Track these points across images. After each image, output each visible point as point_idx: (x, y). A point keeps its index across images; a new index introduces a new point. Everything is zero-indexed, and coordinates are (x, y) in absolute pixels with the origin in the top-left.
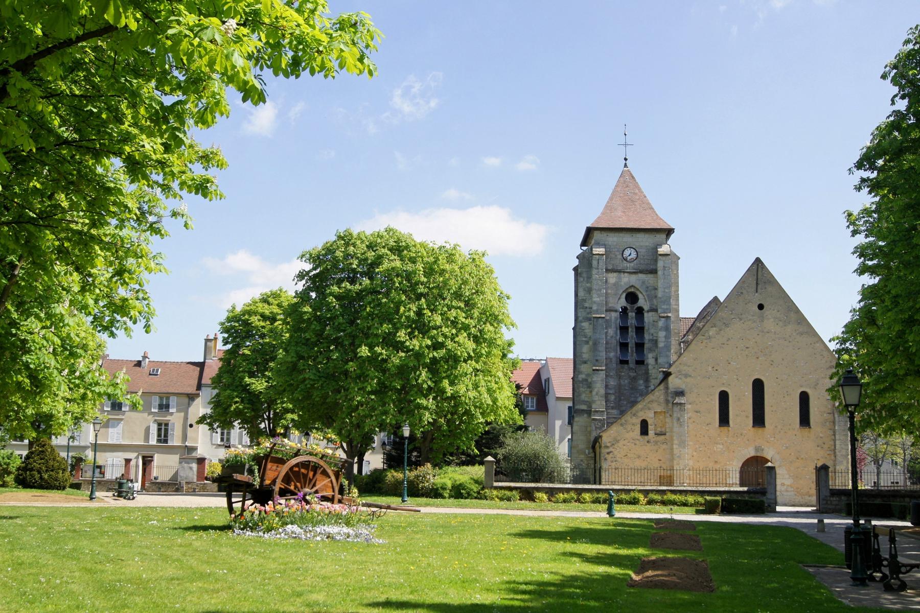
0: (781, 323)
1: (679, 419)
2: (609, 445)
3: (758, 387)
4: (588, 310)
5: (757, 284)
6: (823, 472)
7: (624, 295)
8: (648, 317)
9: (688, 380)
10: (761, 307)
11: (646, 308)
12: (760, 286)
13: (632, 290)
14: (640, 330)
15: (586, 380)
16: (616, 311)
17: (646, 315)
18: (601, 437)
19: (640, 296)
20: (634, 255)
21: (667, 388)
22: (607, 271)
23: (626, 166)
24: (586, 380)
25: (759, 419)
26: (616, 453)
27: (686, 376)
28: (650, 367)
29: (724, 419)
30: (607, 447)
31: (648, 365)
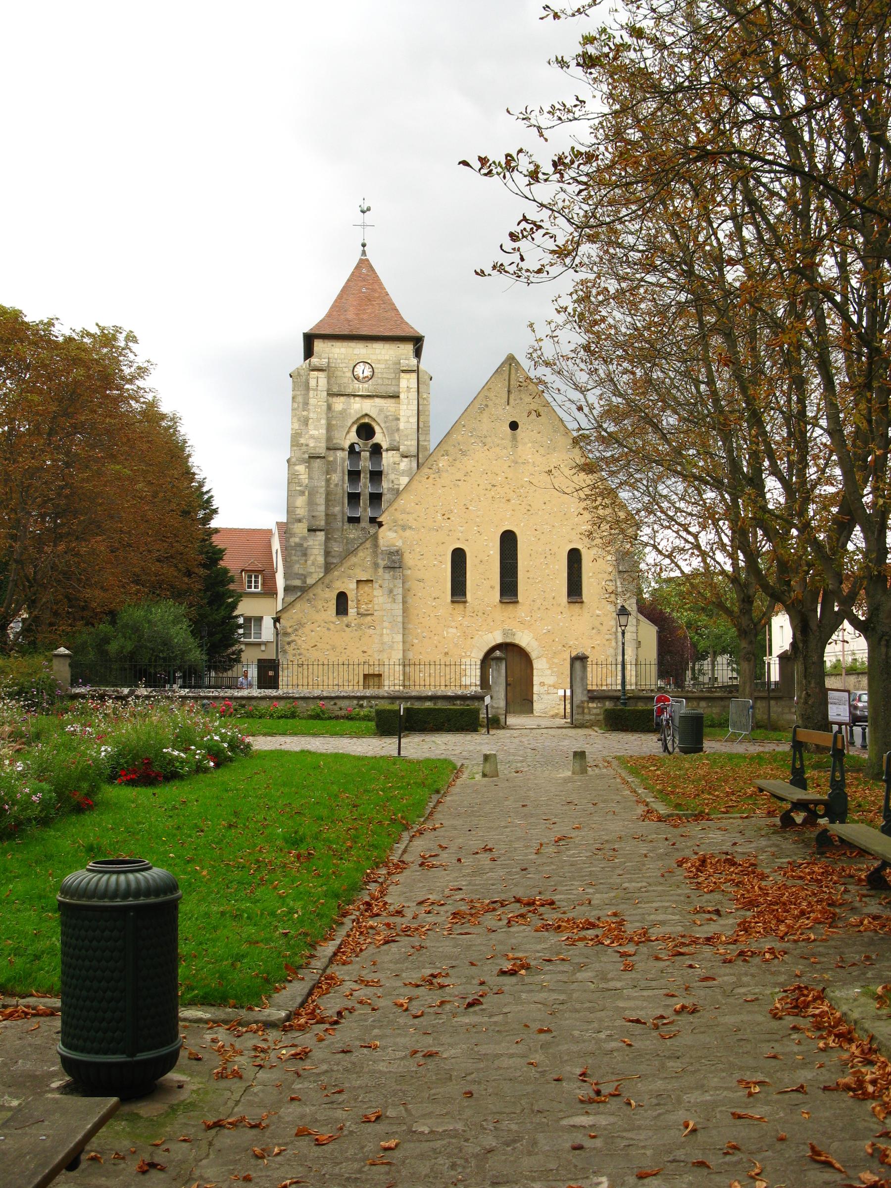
0: (542, 451)
2: (289, 630)
3: (508, 540)
5: (509, 392)
6: (578, 664)
7: (355, 428)
9: (408, 533)
10: (514, 426)
11: (385, 446)
12: (512, 397)
13: (366, 420)
14: (376, 476)
15: (301, 545)
16: (343, 449)
17: (384, 454)
20: (368, 373)
23: (364, 253)
24: (301, 545)
25: (509, 588)
26: (299, 642)
27: (404, 528)
29: (459, 588)
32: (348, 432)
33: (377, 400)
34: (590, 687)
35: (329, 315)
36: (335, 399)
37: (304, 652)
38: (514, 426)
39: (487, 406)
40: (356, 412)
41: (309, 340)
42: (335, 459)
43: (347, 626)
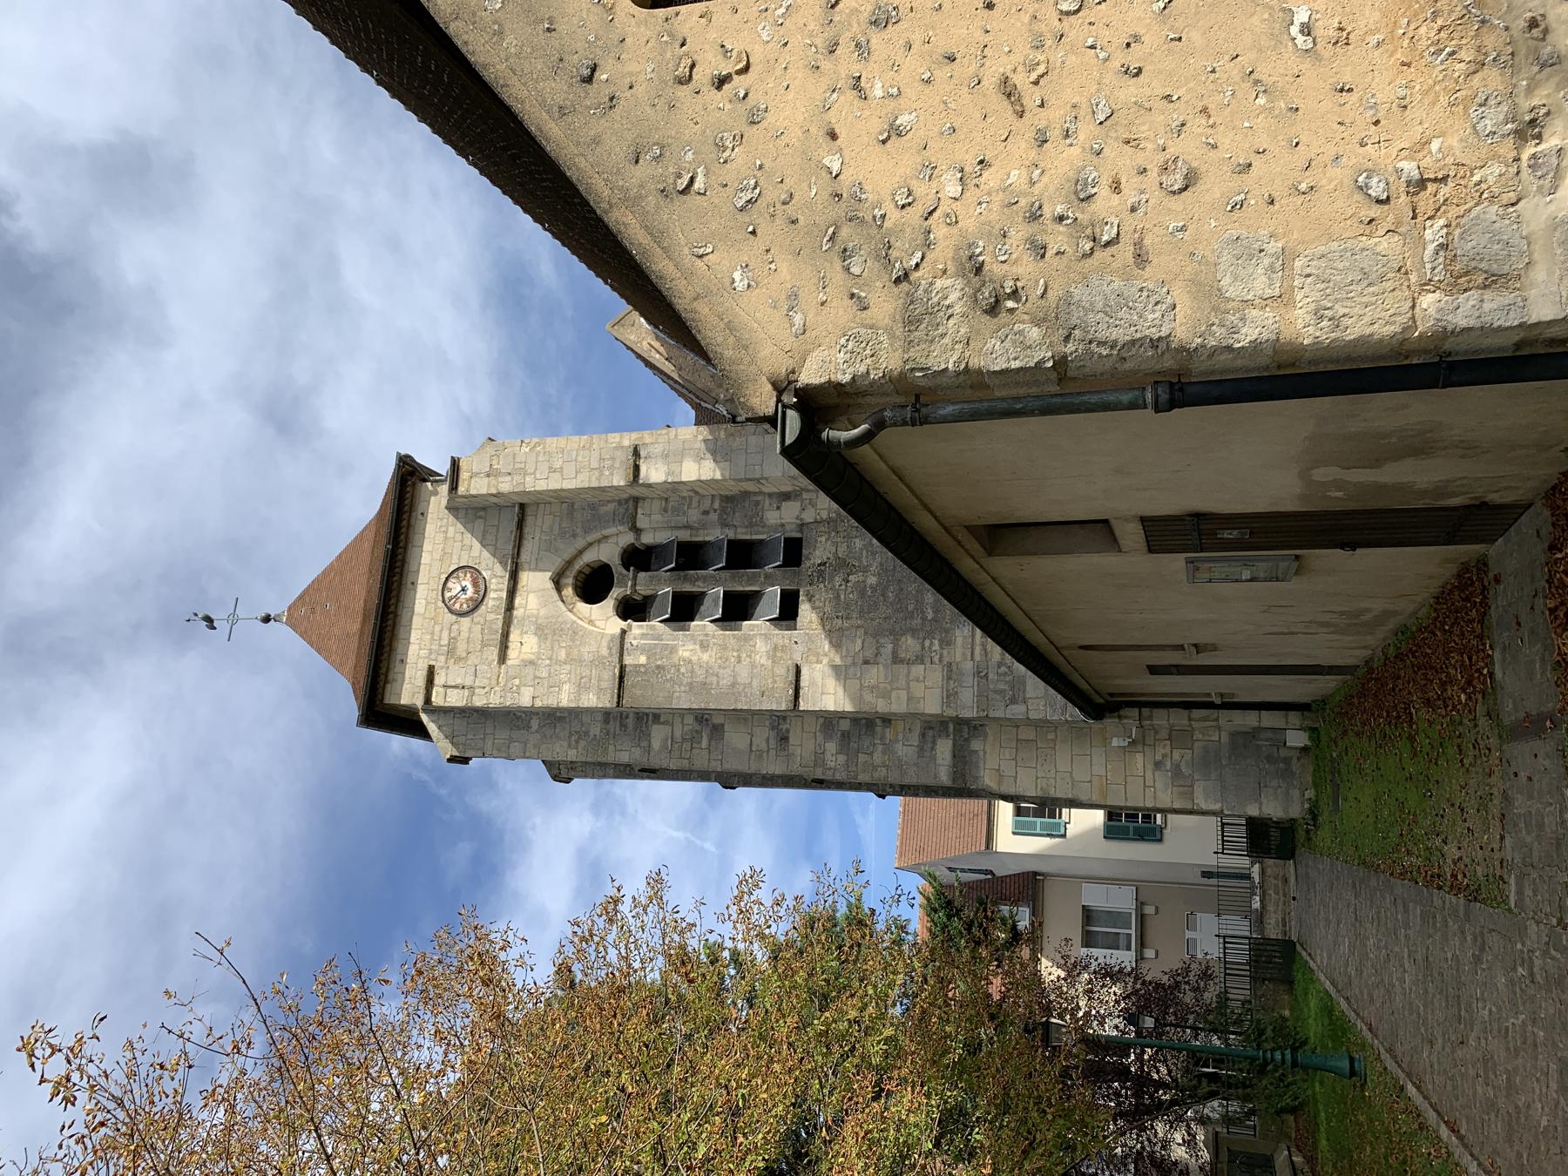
4: (614, 726)
7: (583, 607)
11: (628, 539)
14: (691, 556)
15: (845, 736)
17: (647, 539)
18: (817, 405)
19: (590, 557)
22: (503, 658)
24: (845, 736)
28: (809, 516)
31: (802, 526)
32: (591, 622)
33: (524, 557)
36: (512, 653)
37: (1064, 160)
41: (380, 712)
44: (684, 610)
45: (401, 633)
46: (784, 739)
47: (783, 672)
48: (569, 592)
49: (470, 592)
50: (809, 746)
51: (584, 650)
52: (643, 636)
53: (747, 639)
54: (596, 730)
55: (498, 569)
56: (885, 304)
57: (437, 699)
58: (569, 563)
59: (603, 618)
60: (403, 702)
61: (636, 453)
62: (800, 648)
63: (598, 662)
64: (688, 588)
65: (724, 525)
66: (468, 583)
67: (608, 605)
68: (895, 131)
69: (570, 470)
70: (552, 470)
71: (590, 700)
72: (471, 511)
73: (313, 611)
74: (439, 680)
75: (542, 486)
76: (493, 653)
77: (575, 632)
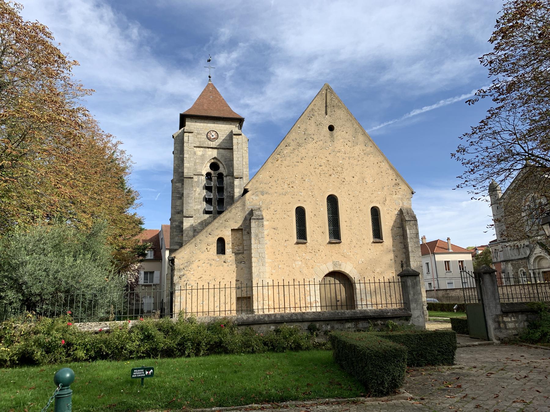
1: (257, 235)
3: (332, 201)
4: (181, 174)
5: (326, 106)
7: (209, 164)
8: (226, 180)
9: (265, 196)
10: (331, 128)
11: (225, 174)
12: (329, 110)
14: (220, 190)
15: (179, 226)
17: (225, 178)
19: (221, 165)
21: (244, 205)
24: (179, 226)
27: (262, 193)
29: (302, 234)
30: (180, 270)
33: (221, 150)
34: (502, 301)
35: (193, 107)
36: (198, 149)
38: (331, 128)
39: (313, 115)
40: (209, 156)
41: (184, 118)
42: (199, 180)
43: (225, 262)
44: (208, 188)
45: (202, 121)
46: (178, 213)
47: (192, 213)
48: (213, 161)
49: (212, 137)
50: (177, 219)
51: (199, 166)
52: (202, 180)
53: (201, 203)
54: (180, 170)
55: (218, 144)
56: (182, 267)
57: (185, 134)
58: (219, 161)
59: (206, 169)
60: (187, 123)
61: (241, 178)
62: (199, 215)
63: (195, 170)
64: (213, 189)
65: (227, 196)
66: (214, 137)
67: (209, 170)
68: (198, 267)
69: (238, 162)
70: (238, 158)
71: (186, 171)
72: (231, 135)
73: (210, 92)
74: (190, 134)
75: (235, 156)
76: (198, 145)
77: (203, 164)
